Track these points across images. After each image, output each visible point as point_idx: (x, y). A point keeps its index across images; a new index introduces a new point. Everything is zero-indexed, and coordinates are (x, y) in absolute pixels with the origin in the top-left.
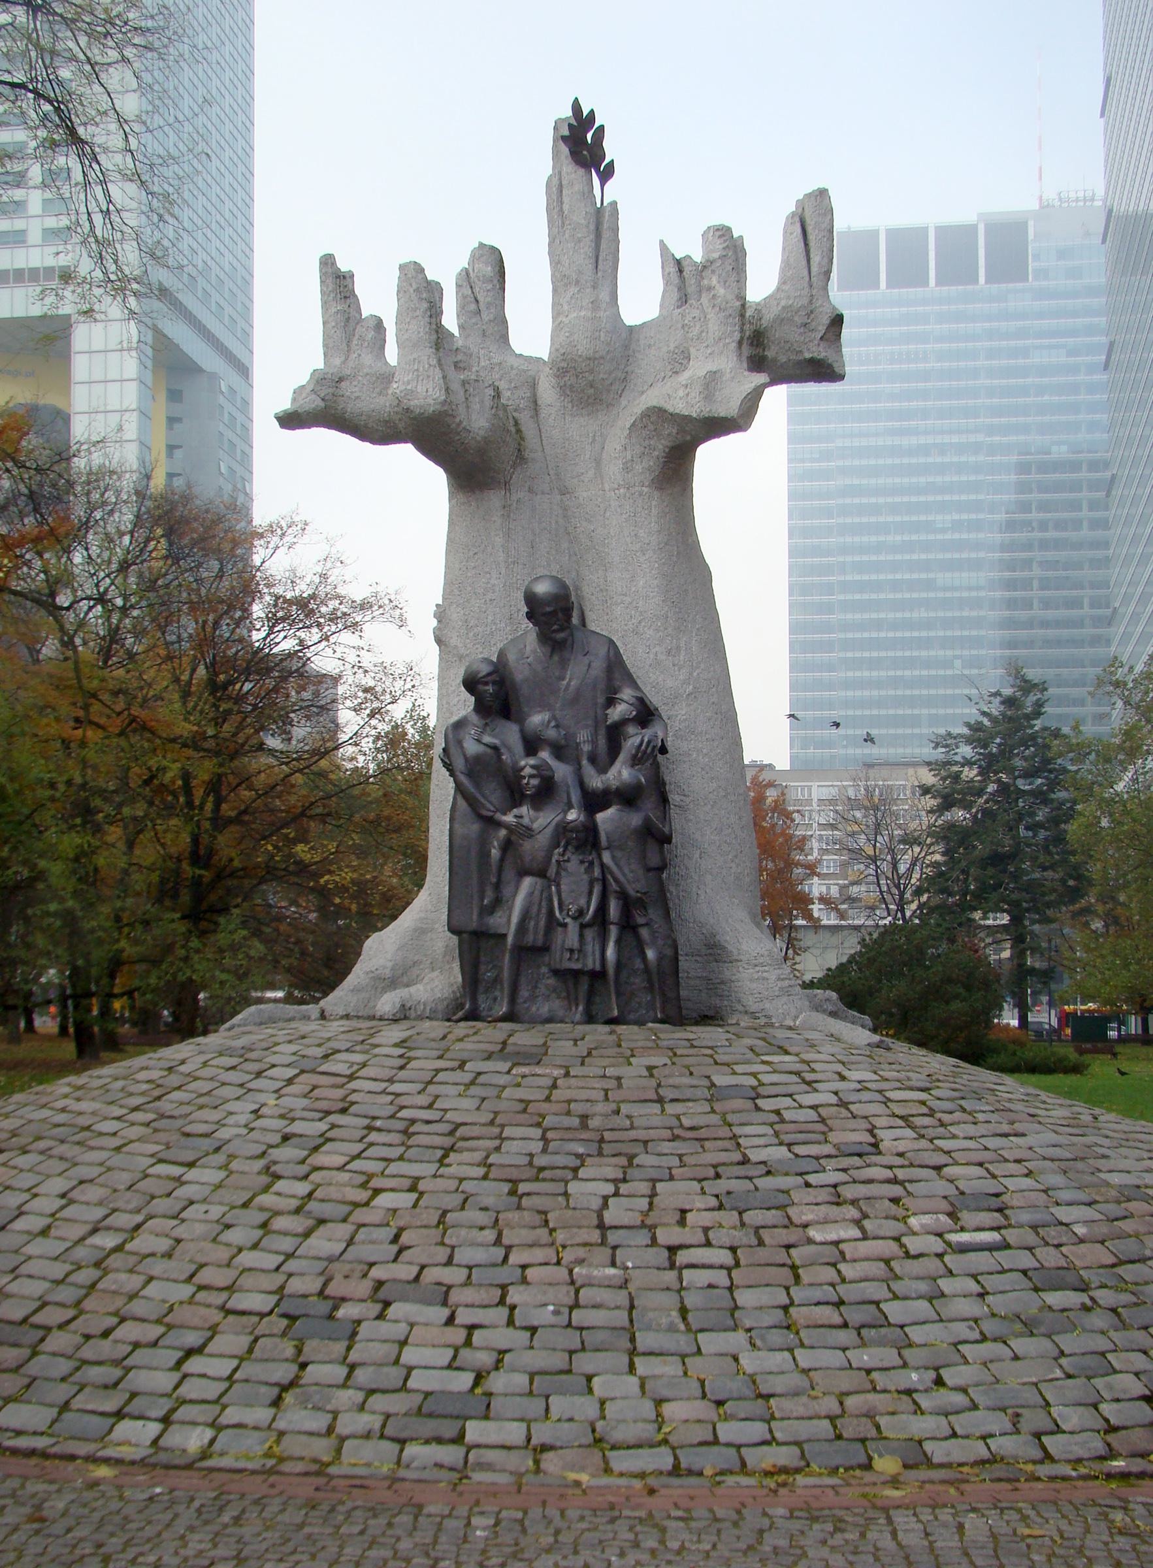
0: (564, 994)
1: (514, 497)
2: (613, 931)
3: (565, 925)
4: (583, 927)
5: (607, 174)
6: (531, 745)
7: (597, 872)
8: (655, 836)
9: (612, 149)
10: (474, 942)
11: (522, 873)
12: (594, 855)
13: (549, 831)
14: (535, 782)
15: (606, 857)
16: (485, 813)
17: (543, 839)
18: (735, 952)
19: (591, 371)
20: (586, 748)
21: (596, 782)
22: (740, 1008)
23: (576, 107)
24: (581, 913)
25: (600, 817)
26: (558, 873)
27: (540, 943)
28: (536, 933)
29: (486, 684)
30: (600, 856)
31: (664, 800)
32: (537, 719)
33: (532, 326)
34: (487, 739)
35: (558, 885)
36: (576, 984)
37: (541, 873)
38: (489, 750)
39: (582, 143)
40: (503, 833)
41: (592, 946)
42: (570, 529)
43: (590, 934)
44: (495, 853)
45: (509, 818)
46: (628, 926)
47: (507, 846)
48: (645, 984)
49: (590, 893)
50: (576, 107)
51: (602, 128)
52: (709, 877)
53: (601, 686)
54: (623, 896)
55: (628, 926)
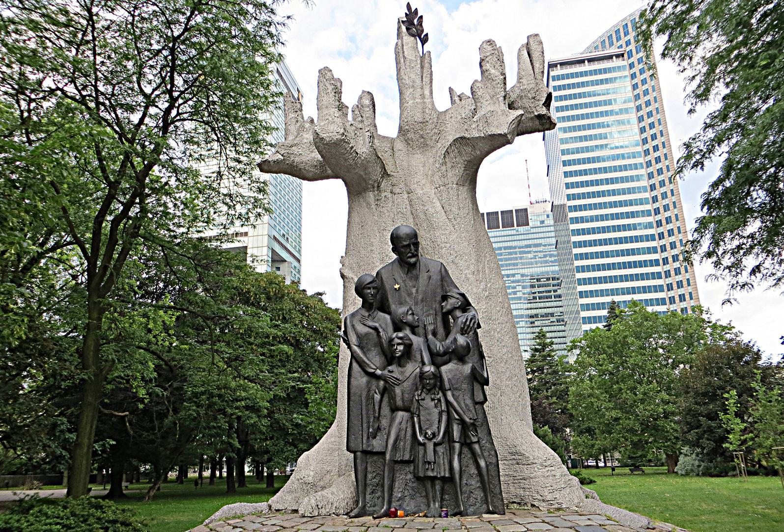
1: (383, 195)
2: (457, 445)
4: (436, 445)
5: (424, 41)
7: (444, 407)
8: (479, 379)
9: (427, 28)
10: (363, 456)
11: (394, 409)
12: (441, 394)
14: (401, 348)
15: (449, 393)
18: (531, 458)
19: (422, 129)
21: (439, 346)
22: (540, 497)
23: (409, 6)
25: (444, 369)
27: (407, 457)
29: (369, 288)
30: (445, 396)
31: (482, 356)
33: (388, 125)
35: (419, 416)
36: (433, 486)
37: (406, 409)
39: (412, 24)
41: (443, 461)
42: (414, 211)
44: (377, 397)
46: (466, 443)
48: (479, 484)
50: (409, 6)
51: (421, 17)
52: (507, 408)
54: (462, 422)
55: (466, 443)
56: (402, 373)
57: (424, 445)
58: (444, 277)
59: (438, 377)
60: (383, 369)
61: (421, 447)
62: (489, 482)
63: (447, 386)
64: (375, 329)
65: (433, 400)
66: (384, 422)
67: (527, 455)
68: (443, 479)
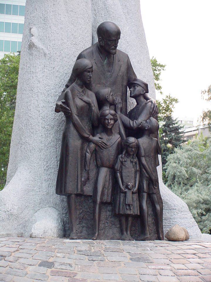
0: (118, 226)
2: (145, 195)
3: (125, 193)
4: (133, 193)
6: (102, 102)
13: (115, 146)
16: (86, 136)
17: (112, 151)
18: (173, 205)
20: (120, 106)
24: (134, 186)
25: (140, 140)
26: (121, 167)
28: (108, 196)
32: (105, 91)
34: (85, 98)
35: (121, 173)
38: (86, 104)
40: (92, 146)
41: (136, 204)
43: (136, 196)
44: (88, 155)
45: (96, 138)
47: (95, 153)
49: (135, 178)
53: (125, 77)
56: (109, 140)
57: (125, 193)
58: (129, 68)
59: (138, 147)
60: (94, 135)
61: (122, 195)
62: (158, 218)
63: (143, 152)
64: (89, 104)
65: (132, 162)
66: (92, 174)
67: (170, 203)
68: (135, 217)
